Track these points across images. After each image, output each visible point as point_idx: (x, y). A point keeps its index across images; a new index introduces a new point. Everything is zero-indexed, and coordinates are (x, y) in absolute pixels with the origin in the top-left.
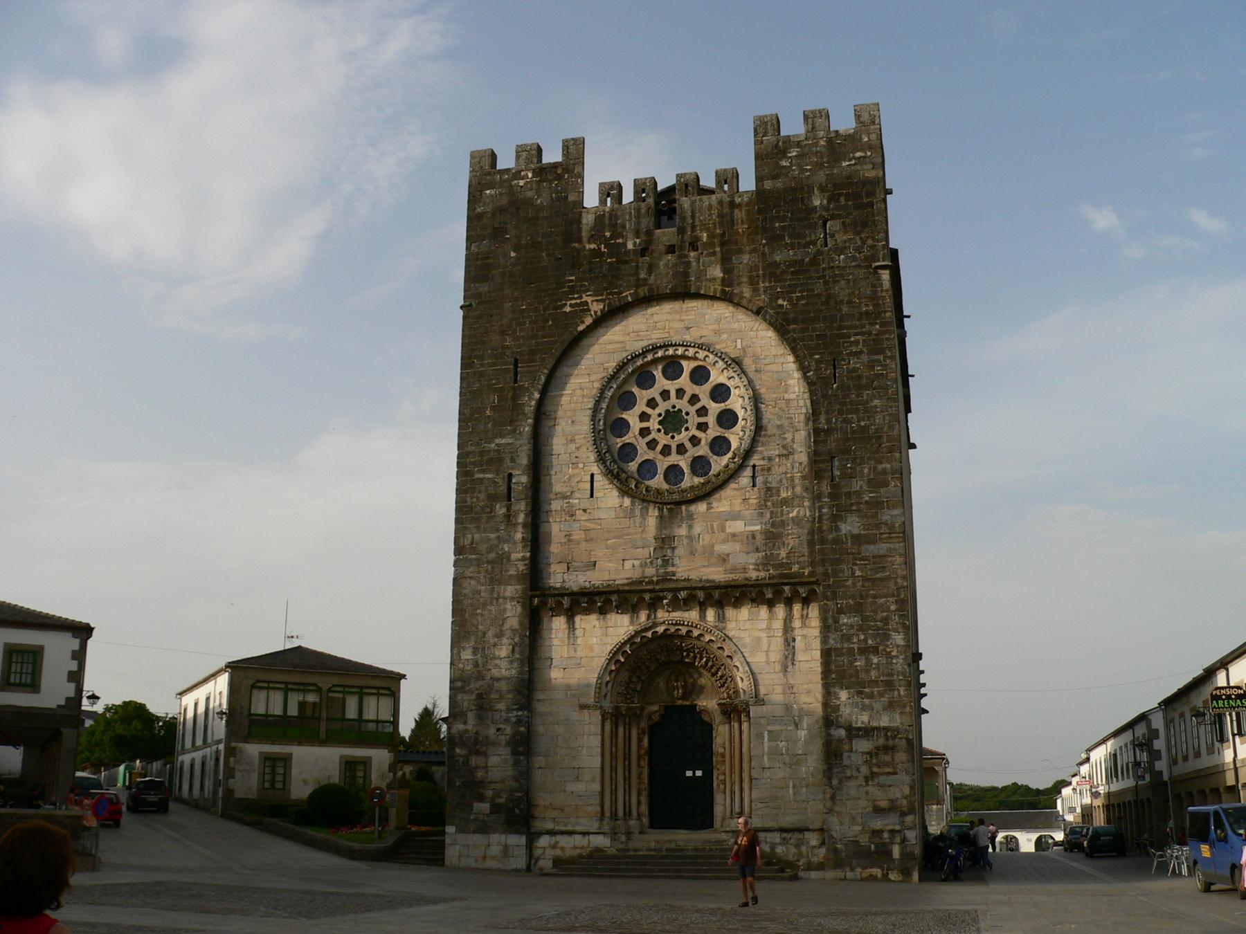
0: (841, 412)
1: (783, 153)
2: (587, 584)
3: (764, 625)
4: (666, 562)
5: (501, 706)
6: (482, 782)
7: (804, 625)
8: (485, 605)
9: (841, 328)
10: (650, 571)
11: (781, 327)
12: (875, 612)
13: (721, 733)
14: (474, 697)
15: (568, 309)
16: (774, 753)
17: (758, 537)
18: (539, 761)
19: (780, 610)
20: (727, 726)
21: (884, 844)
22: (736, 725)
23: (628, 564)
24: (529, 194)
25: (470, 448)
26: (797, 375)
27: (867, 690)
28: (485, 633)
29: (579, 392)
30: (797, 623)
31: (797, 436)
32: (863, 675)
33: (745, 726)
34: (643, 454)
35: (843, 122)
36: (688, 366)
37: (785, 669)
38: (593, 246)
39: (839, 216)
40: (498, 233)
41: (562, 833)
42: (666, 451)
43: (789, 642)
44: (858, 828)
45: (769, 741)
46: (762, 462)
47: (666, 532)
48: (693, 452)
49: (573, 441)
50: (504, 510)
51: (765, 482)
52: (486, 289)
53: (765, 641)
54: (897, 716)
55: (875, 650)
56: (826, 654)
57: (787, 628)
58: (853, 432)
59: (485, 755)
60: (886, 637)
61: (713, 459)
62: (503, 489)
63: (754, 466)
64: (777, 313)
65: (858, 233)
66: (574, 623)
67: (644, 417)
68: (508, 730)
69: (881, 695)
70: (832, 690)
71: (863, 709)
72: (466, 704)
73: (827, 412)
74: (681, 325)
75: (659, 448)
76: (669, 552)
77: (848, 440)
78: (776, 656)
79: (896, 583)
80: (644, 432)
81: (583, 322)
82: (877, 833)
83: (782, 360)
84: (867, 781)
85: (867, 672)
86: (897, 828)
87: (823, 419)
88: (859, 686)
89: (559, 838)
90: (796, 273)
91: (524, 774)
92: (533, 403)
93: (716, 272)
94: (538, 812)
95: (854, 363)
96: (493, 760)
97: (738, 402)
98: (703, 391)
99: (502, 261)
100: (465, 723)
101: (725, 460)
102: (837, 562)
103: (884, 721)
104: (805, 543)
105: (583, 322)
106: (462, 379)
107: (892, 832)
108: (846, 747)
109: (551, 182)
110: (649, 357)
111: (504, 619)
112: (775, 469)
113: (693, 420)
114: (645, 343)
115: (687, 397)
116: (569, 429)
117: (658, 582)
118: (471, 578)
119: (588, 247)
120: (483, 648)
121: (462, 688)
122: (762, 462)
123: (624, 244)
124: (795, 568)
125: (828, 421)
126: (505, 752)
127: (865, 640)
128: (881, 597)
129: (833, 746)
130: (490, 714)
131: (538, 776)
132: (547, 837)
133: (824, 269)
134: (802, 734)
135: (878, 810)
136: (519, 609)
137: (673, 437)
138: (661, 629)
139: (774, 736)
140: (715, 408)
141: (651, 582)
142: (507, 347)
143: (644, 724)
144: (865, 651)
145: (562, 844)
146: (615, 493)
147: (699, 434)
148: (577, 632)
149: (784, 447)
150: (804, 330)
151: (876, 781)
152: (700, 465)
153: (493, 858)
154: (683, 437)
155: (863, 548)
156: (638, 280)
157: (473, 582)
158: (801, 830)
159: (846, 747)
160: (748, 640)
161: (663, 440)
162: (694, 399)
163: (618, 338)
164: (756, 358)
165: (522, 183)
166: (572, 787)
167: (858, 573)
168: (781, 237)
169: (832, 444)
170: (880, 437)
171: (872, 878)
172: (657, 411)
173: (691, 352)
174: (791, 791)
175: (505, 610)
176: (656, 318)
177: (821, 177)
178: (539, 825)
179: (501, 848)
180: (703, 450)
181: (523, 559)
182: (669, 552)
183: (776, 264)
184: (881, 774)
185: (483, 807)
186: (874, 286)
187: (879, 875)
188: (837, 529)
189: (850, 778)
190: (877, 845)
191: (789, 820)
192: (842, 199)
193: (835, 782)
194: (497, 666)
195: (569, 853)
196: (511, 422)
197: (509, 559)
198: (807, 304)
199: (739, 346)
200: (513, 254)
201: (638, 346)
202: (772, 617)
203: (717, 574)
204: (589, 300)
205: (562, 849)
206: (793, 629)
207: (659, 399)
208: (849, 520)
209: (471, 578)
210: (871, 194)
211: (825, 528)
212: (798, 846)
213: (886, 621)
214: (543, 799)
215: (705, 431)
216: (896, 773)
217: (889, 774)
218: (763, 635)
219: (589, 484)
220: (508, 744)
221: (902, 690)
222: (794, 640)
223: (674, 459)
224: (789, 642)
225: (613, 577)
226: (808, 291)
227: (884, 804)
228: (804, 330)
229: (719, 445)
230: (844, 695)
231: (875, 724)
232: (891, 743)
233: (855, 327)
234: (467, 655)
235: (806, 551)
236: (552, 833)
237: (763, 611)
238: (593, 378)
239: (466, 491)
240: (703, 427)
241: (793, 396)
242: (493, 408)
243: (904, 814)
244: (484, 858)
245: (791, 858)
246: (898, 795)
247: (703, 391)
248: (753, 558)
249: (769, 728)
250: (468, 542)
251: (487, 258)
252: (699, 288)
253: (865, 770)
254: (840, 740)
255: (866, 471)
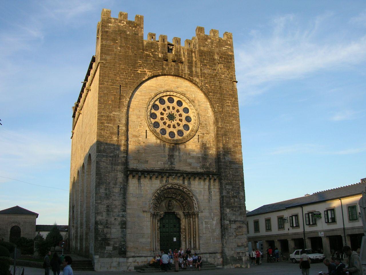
0: (225, 123)
1: (206, 40)
2: (145, 169)
3: (202, 187)
4: (172, 163)
5: (116, 210)
6: (109, 239)
7: (214, 188)
8: (109, 172)
9: (224, 97)
10: (167, 166)
11: (206, 95)
12: (236, 185)
13: (184, 222)
14: (105, 206)
15: (140, 72)
16: (206, 228)
17: (200, 158)
18: (128, 231)
19: (207, 182)
20: (187, 220)
21: (240, 257)
22: (191, 219)
23: (159, 163)
24: (125, 29)
25: (102, 114)
26: (210, 109)
27: (234, 209)
28: (109, 183)
29: (141, 101)
30: (212, 187)
31: (211, 128)
32: (233, 204)
33: (196, 219)
34: (162, 126)
35: (221, 35)
36: (176, 99)
37: (209, 201)
38: (147, 53)
39: (222, 63)
40: (114, 40)
41: (138, 257)
42: (169, 126)
43: (210, 193)
44: (234, 252)
45: (205, 224)
46: (201, 135)
47: (171, 154)
48: (178, 128)
49: (139, 118)
50: (116, 139)
51: (202, 141)
52: (109, 58)
53: (203, 192)
54: (242, 217)
55: (236, 197)
56: (222, 198)
57: (209, 189)
58: (228, 130)
59: (110, 228)
60: (239, 193)
61: (184, 131)
62: (116, 130)
63: (198, 135)
64: (206, 89)
65: (228, 70)
66: (140, 181)
67: (162, 114)
68: (119, 219)
69: (238, 211)
70: (225, 209)
71: (233, 215)
72: (102, 209)
73: (221, 122)
74: (175, 86)
75: (167, 125)
76: (173, 160)
77: (227, 131)
78: (206, 197)
79: (241, 177)
80: (162, 119)
81: (144, 77)
82: (238, 253)
83: (206, 103)
84: (235, 237)
85: (234, 203)
86: (244, 251)
87: (220, 124)
88: (232, 208)
89: (136, 258)
90: (210, 77)
91: (124, 236)
92: (127, 102)
93: (187, 71)
94: (128, 250)
95: (228, 109)
96: (113, 230)
97: (191, 114)
98: (181, 109)
99: (115, 50)
100: (102, 216)
101: (188, 132)
102: (226, 169)
103: (239, 219)
104: (214, 162)
105: (144, 77)
106: (99, 88)
107: (242, 253)
108: (229, 227)
109: (133, 27)
110: (165, 94)
111: (117, 178)
112: (205, 137)
113: (178, 118)
114: (164, 89)
115: (176, 110)
116: (138, 113)
117: (169, 170)
118: (103, 162)
119: (145, 52)
120: (109, 189)
121: (101, 203)
122: (201, 135)
123: (158, 55)
124: (211, 169)
125: (221, 125)
126: (119, 227)
127: (233, 194)
128: (237, 181)
129: (226, 226)
130: (112, 213)
131: (128, 237)
132: (132, 258)
133: (219, 78)
134: (215, 222)
135: (238, 246)
136: (123, 175)
137: (171, 122)
138: (169, 186)
139: (206, 223)
140: (184, 115)
141: (167, 170)
142: (117, 80)
143: (158, 218)
144: (233, 197)
145: (138, 261)
146: (155, 138)
147: (180, 122)
148: (142, 185)
149: (207, 131)
150: (214, 96)
151: (238, 237)
152: (180, 133)
153: (114, 267)
154: (175, 122)
155: (232, 165)
156: (163, 68)
157: (105, 164)
158: (215, 253)
159: (229, 227)
160: (198, 191)
161: (168, 122)
162: (178, 111)
163: (154, 86)
164: (199, 101)
165: (122, 25)
166: (140, 240)
167: (231, 173)
168: (205, 65)
169: (222, 132)
170: (235, 132)
171: (237, 267)
172: (166, 112)
173: (178, 95)
174: (212, 240)
175: (117, 175)
176: (167, 82)
177: (217, 50)
178: (128, 254)
179: (117, 263)
180: (181, 128)
181: (124, 157)
182: (173, 160)
183: (204, 73)
184: (239, 235)
185: (109, 248)
186: (232, 87)
187: (239, 267)
188: (225, 159)
189: (231, 236)
190: (238, 258)
191: (211, 250)
192: (223, 58)
193: (226, 237)
194: (114, 195)
195: (141, 264)
196: (119, 107)
197: (118, 156)
198: (214, 88)
199: (193, 97)
200: (119, 48)
201: (162, 90)
202: (205, 184)
203: (188, 169)
204: (147, 70)
205: (138, 262)
206: (211, 189)
207: (166, 109)
208: (228, 156)
209: (103, 162)
210: (231, 59)
211: (221, 158)
212: (214, 258)
213: (239, 188)
214: (130, 245)
215: (181, 121)
216: (243, 235)
217: (241, 235)
218: (202, 190)
219: (145, 133)
220: (119, 224)
221: (243, 209)
222: (211, 192)
223: (172, 129)
224: (210, 193)
225: (154, 167)
226: (214, 84)
227: (240, 244)
228: (214, 96)
229: (186, 127)
230: (228, 210)
231: (236, 220)
232: (241, 225)
233: (228, 98)
234: (102, 190)
235: (214, 164)
236: (133, 257)
237: (202, 183)
238: (146, 97)
239: (102, 129)
240: (181, 120)
241: (209, 115)
242: (112, 101)
243: (245, 247)
244: (111, 267)
245: (212, 262)
246: (244, 241)
247: (181, 109)
248: (199, 165)
249: (205, 220)
250: (102, 148)
251: (109, 47)
252: (182, 75)
253: (234, 234)
254: (228, 224)
255: (232, 142)
